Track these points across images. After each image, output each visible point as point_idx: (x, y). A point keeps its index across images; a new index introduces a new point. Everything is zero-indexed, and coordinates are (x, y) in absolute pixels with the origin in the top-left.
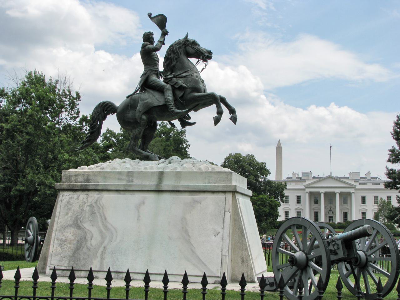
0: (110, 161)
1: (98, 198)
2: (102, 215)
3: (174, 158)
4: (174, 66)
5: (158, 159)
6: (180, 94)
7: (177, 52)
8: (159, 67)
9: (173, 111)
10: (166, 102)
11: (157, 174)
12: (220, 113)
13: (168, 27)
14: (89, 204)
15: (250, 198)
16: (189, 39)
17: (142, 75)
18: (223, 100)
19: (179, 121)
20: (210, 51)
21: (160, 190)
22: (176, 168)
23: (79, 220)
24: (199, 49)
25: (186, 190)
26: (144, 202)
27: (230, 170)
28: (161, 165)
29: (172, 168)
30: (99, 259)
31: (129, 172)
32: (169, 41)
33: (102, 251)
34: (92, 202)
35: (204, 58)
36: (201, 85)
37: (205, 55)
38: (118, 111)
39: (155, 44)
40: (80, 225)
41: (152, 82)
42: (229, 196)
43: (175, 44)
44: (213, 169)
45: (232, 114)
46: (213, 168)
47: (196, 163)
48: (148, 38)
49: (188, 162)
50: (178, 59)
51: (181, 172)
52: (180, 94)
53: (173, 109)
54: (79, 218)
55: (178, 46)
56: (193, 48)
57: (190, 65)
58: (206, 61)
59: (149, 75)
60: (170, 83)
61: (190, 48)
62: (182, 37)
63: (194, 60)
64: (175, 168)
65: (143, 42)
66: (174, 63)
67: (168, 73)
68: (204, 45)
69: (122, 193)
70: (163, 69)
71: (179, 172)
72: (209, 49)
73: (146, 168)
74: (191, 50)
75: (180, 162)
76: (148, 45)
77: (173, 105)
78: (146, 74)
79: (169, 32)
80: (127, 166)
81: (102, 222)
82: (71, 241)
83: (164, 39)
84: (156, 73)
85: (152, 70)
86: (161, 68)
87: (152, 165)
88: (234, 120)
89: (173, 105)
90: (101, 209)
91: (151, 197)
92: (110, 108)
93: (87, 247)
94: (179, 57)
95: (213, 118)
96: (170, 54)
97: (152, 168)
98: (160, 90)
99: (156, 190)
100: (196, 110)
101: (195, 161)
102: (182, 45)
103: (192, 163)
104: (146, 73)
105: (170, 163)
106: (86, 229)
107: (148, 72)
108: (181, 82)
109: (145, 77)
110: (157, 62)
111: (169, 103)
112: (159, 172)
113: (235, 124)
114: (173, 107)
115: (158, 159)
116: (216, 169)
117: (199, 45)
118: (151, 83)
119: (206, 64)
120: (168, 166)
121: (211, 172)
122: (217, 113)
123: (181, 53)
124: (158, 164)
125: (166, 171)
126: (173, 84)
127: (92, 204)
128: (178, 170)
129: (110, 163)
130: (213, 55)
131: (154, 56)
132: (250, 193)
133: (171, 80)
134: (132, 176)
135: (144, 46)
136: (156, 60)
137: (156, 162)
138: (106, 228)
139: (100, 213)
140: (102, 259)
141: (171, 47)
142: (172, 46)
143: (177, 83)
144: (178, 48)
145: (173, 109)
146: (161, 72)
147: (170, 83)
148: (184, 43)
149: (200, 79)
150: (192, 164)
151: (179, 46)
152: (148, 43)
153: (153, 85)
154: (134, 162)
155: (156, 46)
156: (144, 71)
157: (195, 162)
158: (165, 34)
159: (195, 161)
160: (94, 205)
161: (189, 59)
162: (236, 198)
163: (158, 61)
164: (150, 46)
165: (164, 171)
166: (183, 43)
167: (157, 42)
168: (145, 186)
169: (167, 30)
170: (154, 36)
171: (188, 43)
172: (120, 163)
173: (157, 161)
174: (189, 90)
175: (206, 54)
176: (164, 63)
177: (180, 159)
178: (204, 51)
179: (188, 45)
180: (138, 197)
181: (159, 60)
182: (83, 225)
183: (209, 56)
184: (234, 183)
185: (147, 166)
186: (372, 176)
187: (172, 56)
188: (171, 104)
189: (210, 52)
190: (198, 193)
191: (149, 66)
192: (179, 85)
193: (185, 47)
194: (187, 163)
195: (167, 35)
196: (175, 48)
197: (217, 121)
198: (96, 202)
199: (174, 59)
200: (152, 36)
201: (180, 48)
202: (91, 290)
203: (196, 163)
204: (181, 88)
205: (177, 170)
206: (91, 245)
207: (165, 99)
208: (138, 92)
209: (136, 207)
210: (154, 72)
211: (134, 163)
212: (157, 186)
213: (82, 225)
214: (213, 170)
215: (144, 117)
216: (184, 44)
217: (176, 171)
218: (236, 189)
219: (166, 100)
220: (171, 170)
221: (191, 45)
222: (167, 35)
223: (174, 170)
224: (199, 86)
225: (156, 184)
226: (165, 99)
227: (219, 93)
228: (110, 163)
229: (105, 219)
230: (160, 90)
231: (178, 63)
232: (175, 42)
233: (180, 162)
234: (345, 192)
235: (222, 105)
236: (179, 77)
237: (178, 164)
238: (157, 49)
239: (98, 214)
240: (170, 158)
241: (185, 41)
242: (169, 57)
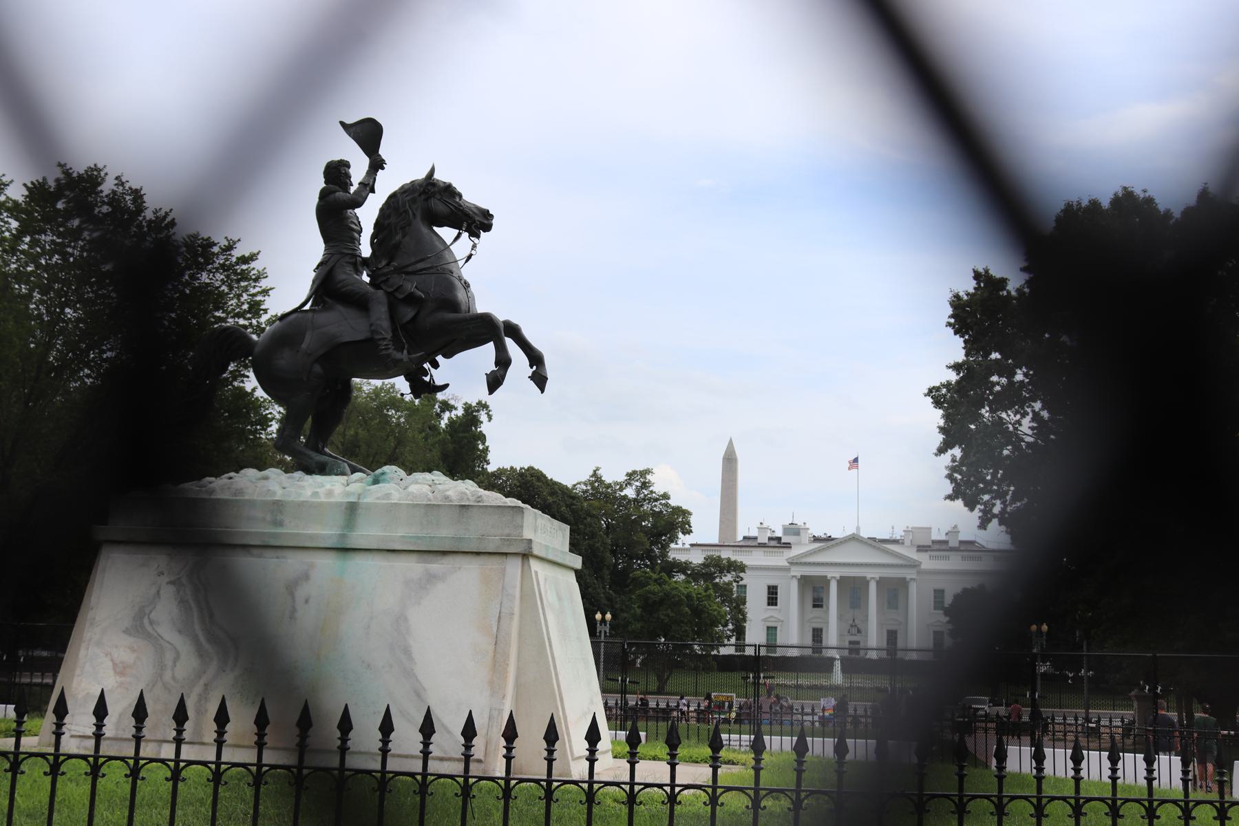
0: (232, 474)
3: (388, 471)
4: (397, 246)
5: (348, 470)
6: (408, 313)
7: (406, 212)
8: (360, 247)
9: (388, 356)
10: (373, 332)
12: (503, 362)
13: (383, 151)
15: (575, 573)
16: (438, 180)
17: (318, 266)
18: (513, 331)
19: (407, 380)
20: (488, 211)
21: (348, 547)
22: (391, 494)
23: (147, 617)
24: (461, 206)
25: (412, 549)
26: (307, 577)
27: (519, 503)
28: (356, 487)
29: (379, 495)
32: (388, 184)
33: (200, 695)
35: (471, 227)
36: (461, 295)
37: (474, 222)
38: (257, 349)
39: (352, 189)
40: (149, 628)
41: (340, 282)
42: (514, 566)
43: (402, 190)
44: (480, 499)
45: (535, 368)
46: (479, 497)
47: (439, 484)
48: (336, 173)
49: (420, 481)
50: (407, 228)
51: (401, 504)
52: (408, 313)
53: (390, 351)
54: (147, 612)
55: (408, 198)
56: (445, 203)
57: (437, 243)
58: (478, 237)
59: (334, 266)
60: (384, 287)
61: (437, 201)
62: (421, 175)
63: (446, 233)
64: (388, 496)
65: (324, 185)
66: (398, 237)
67: (380, 262)
68: (472, 195)
70: (371, 251)
71: (396, 504)
72: (484, 206)
73: (317, 492)
74: (438, 206)
75: (401, 480)
76: (335, 192)
77: (390, 340)
78: (328, 263)
79: (386, 162)
80: (270, 488)
82: (124, 668)
83: (375, 179)
84: (353, 260)
85: (342, 253)
86: (366, 250)
87: (334, 485)
88: (540, 380)
89: (390, 340)
93: (163, 684)
94: (410, 225)
95: (486, 374)
96: (389, 216)
97: (330, 493)
98: (358, 302)
99: (339, 546)
100: (448, 355)
101: (438, 480)
102: (420, 195)
103: (430, 483)
104: (327, 262)
105: (376, 481)
106: (162, 638)
107: (332, 259)
108: (411, 286)
109: (327, 268)
110: (356, 235)
111: (381, 337)
112: (348, 502)
113: (542, 391)
114: (390, 346)
115: (349, 472)
116: (485, 498)
117: (460, 196)
118: (339, 285)
119: (476, 240)
120: (369, 490)
122: (497, 364)
123: (414, 214)
124: (348, 485)
125: (365, 501)
126: (390, 290)
128: (394, 500)
129: (230, 478)
130: (494, 222)
131: (350, 220)
132: (577, 562)
133: (387, 280)
135: (324, 195)
136: (353, 230)
137: (342, 479)
140: (198, 713)
141: (393, 200)
142: (393, 197)
143: (401, 286)
144: (408, 201)
145: (390, 351)
146: (365, 260)
147: (383, 286)
148: (424, 190)
149: (460, 279)
150: (430, 486)
151: (412, 196)
152: (337, 188)
153: (344, 289)
154: (289, 478)
155: (354, 196)
156: (324, 255)
157: (438, 482)
158: (377, 164)
159: (438, 480)
161: (435, 228)
162: (530, 569)
163: (360, 232)
164: (340, 194)
165: (360, 501)
166: (422, 189)
167: (358, 186)
168: (312, 537)
169: (383, 157)
170: (352, 171)
171: (432, 190)
172: (254, 481)
173: (345, 477)
175: (477, 218)
176: (373, 237)
177: (402, 473)
178: (472, 211)
179: (433, 195)
181: (361, 229)
183: (484, 224)
184: (527, 534)
185: (320, 487)
186: (962, 537)
187: (393, 220)
188: (384, 339)
189: (487, 215)
190: (439, 558)
191: (336, 244)
192: (406, 294)
193: (426, 200)
194: (417, 483)
195: (383, 168)
196: (400, 203)
197: (494, 382)
199: (398, 228)
200: (347, 169)
201: (414, 201)
202: (60, 738)
203: (439, 484)
204: (411, 299)
205: (391, 499)
206: (174, 678)
207: (371, 325)
208: (307, 307)
209: (287, 588)
210: (347, 259)
211: (290, 480)
212: (343, 536)
213: (154, 629)
215: (317, 368)
216: (424, 192)
217: (390, 501)
218: (531, 548)
219: (373, 328)
220: (378, 498)
221: (441, 194)
222: (383, 168)
223: (384, 499)
224: (455, 296)
225: (338, 533)
226: (371, 325)
227: (501, 315)
228: (230, 478)
230: (358, 302)
231: (407, 238)
232: (403, 187)
233: (401, 480)
234: (190, 482)
235: (510, 343)
236: (408, 273)
237: (397, 486)
238: (358, 202)
240: (379, 471)
241: (427, 185)
242: (386, 222)
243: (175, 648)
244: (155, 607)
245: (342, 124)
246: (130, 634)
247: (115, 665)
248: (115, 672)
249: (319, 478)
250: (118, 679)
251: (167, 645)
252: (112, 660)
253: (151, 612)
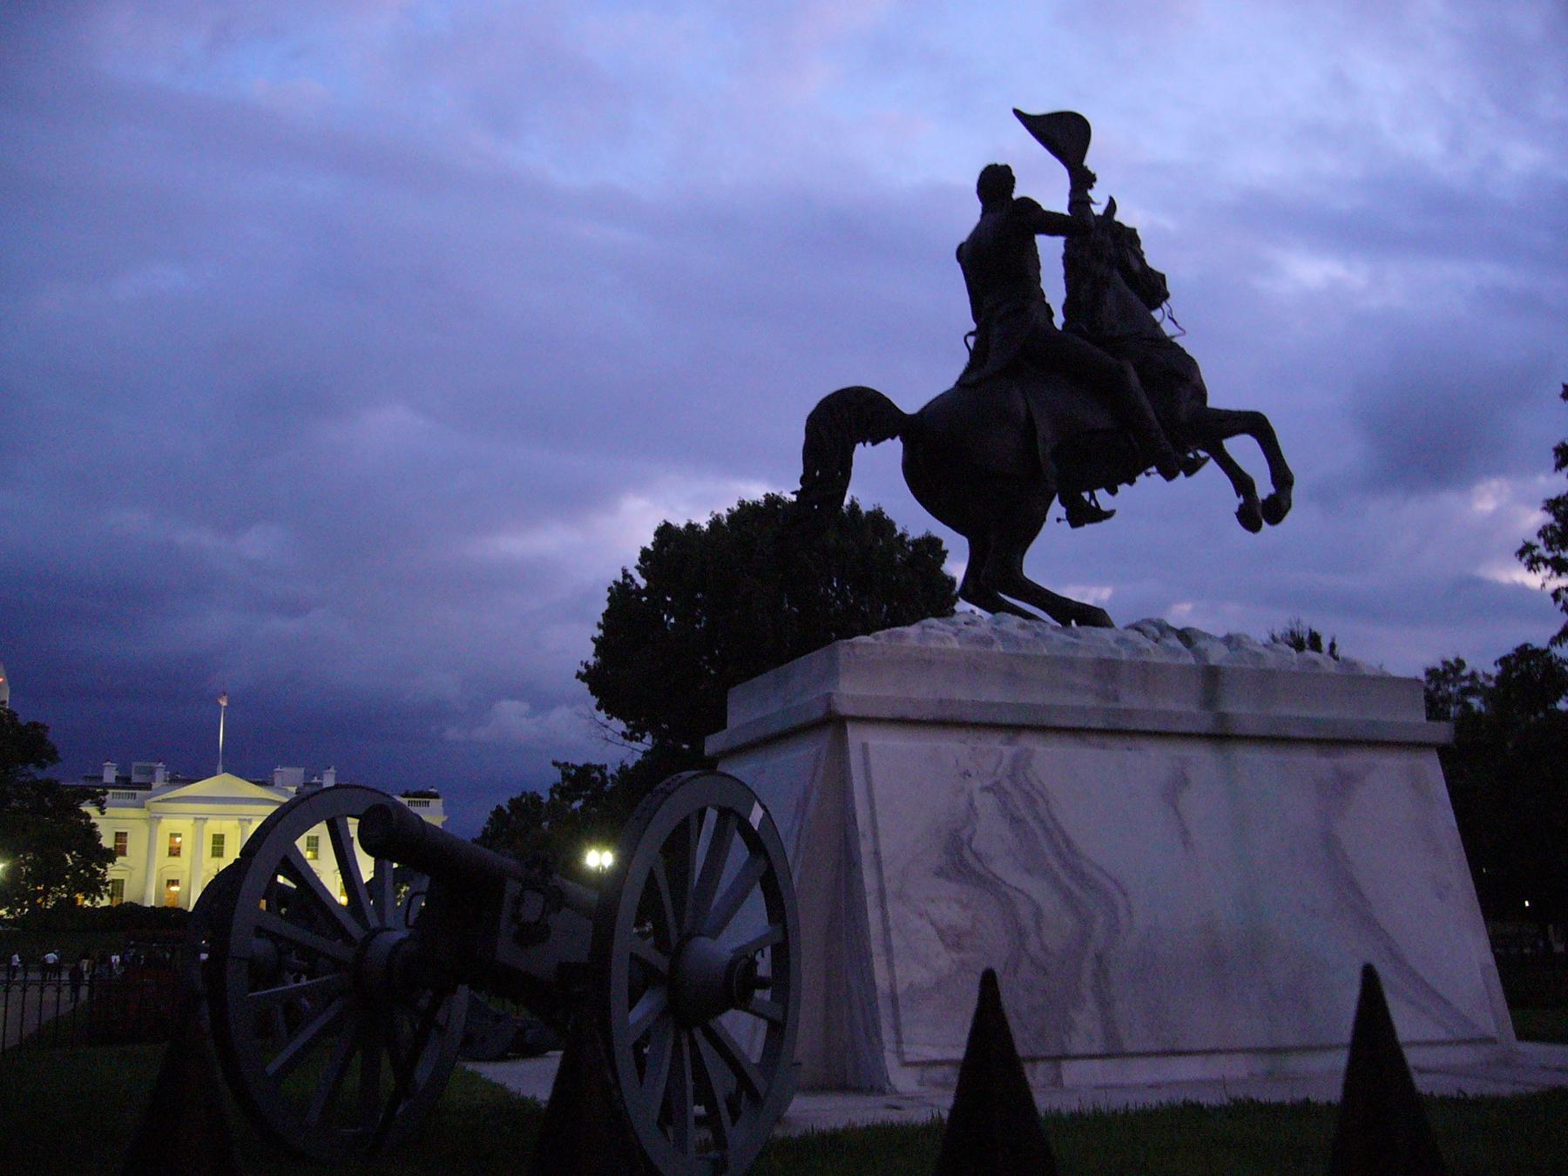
1: (1016, 758)
2: (1050, 825)
13: (1090, 162)
14: (988, 782)
26: (1185, 779)
30: (1091, 1006)
34: (995, 773)
40: (977, 866)
69: (1095, 739)
81: (1059, 854)
90: (1040, 801)
91: (1201, 757)
122: (1274, 482)
127: (997, 783)
138: (1081, 877)
139: (1042, 821)
160: (1007, 784)
180: (1156, 759)
182: (992, 867)
198: (1012, 777)
206: (1044, 948)
229: (1068, 841)
239: (1033, 824)
243: (1029, 897)
244: (975, 831)
245: (1017, 113)
246: (948, 878)
247: (940, 932)
248: (947, 946)
249: (1098, 629)
250: (955, 956)
251: (1018, 894)
252: (933, 924)
253: (970, 839)
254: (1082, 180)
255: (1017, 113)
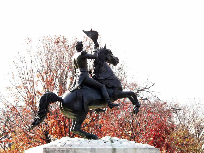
6: (111, 91)
11: (112, 150)
13: (98, 41)
31: (92, 149)
41: (89, 81)
92: (55, 98)
111: (108, 99)
117: (112, 54)
118: (89, 82)
121: (145, 149)
126: (106, 84)
134: (94, 151)
153: (91, 83)
174: (117, 89)
204: (113, 87)
214: (146, 147)
254: (97, 45)
255: (83, 31)
